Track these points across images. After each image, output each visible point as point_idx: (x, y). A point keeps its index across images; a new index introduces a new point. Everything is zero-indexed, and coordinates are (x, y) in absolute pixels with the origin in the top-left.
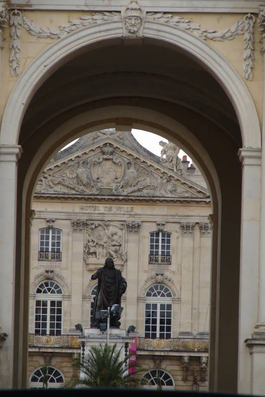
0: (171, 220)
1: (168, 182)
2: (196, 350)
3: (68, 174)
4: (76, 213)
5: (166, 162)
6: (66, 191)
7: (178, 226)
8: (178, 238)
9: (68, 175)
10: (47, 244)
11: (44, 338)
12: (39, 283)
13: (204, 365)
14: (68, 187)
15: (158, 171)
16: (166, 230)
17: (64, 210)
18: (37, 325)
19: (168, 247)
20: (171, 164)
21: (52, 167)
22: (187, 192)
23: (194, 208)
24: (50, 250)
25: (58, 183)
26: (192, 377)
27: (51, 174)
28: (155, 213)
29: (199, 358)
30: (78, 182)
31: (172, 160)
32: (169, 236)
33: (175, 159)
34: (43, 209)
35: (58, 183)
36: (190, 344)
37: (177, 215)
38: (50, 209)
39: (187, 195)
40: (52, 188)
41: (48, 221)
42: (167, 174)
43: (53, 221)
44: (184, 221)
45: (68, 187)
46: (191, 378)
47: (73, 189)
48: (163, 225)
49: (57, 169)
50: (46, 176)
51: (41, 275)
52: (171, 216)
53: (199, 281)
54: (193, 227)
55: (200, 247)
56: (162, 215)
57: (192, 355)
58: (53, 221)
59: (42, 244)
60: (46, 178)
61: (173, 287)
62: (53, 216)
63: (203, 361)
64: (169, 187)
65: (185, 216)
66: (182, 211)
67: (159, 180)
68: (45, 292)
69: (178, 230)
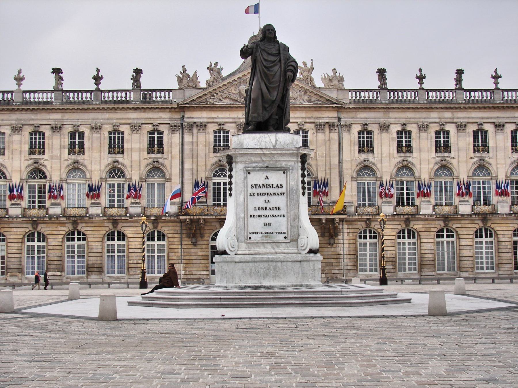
0: (308, 121)
1: (305, 94)
2: (331, 213)
3: (233, 90)
4: (239, 118)
5: (303, 80)
6: (232, 102)
7: (313, 125)
8: (313, 134)
9: (233, 91)
10: (220, 141)
11: (219, 209)
12: (214, 169)
13: (337, 224)
14: (233, 100)
15: (297, 86)
16: (304, 128)
17: (231, 116)
18: (214, 200)
19: (307, 141)
20: (306, 81)
21: (221, 85)
22: (319, 100)
23: (324, 112)
24: (222, 145)
25: (226, 97)
26: (328, 234)
27: (221, 91)
28: (296, 116)
29: (334, 219)
30: (240, 96)
31: (307, 79)
32: (307, 132)
33: (309, 78)
34: (216, 116)
35: (226, 97)
36: (327, 209)
37: (312, 117)
38: (220, 116)
39: (319, 103)
40: (222, 100)
41: (219, 125)
42: (304, 88)
43: (223, 125)
44: (318, 121)
45: (233, 100)
46: (327, 234)
47: (237, 101)
48: (303, 124)
49: (225, 87)
50: (217, 92)
51: (216, 163)
52: (308, 118)
53: (330, 164)
54: (324, 125)
55: (330, 140)
56: (301, 118)
57: (328, 217)
58: (223, 125)
59: (216, 141)
60: (217, 94)
61: (311, 169)
62: (224, 121)
63: (336, 222)
64: (306, 98)
65: (318, 118)
66: (316, 114)
67: (299, 93)
68: (219, 176)
69: (314, 128)
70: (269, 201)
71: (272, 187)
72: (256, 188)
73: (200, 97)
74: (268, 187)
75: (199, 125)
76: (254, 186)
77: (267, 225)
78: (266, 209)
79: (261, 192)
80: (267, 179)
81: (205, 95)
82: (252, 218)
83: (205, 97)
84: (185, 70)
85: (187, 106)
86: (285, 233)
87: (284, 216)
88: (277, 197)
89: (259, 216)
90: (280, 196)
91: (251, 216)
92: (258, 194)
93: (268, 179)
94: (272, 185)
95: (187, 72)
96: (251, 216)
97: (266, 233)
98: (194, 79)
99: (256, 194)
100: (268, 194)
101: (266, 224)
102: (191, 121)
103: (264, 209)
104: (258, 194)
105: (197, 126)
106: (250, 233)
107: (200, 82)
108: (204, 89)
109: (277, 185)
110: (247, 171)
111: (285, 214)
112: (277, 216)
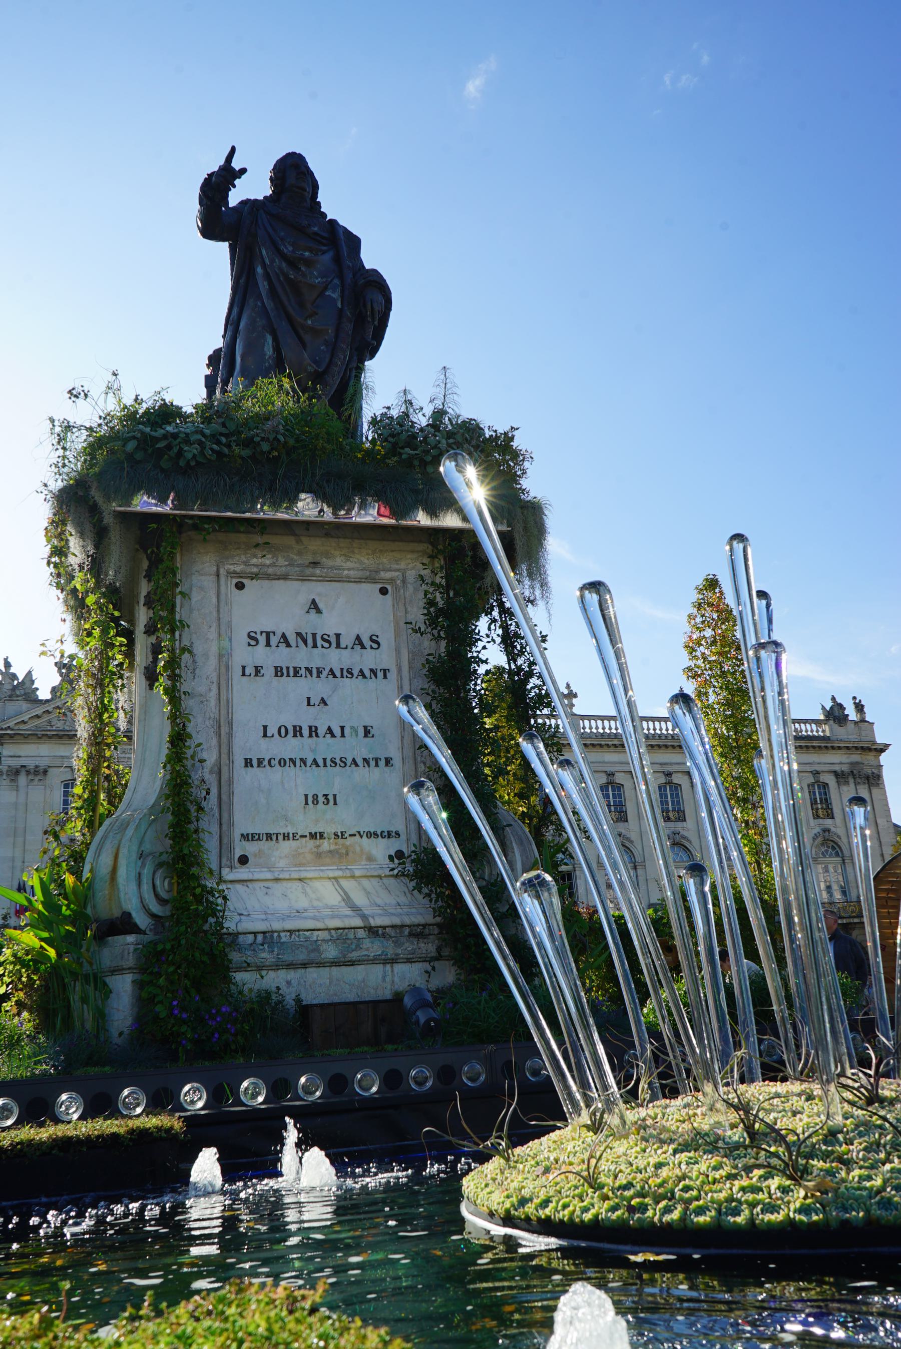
70: (324, 702)
71: (338, 646)
72: (268, 644)
73: (38, 716)
74: (319, 642)
75: (32, 771)
76: (262, 639)
77: (321, 799)
78: (313, 731)
79: (291, 666)
80: (313, 611)
81: (48, 712)
82: (255, 770)
83: (46, 718)
84: (7, 665)
85: (9, 732)
86: (398, 834)
87: (388, 762)
88: (356, 683)
89: (282, 763)
90: (372, 683)
91: (248, 763)
92: (278, 672)
93: (319, 611)
94: (338, 636)
95: (12, 670)
96: (248, 763)
97: (313, 836)
98: (28, 684)
99: (268, 672)
100: (319, 672)
101: (315, 797)
102: (16, 763)
103: (306, 732)
104: (278, 672)
105: (28, 772)
106: (245, 837)
107: (37, 689)
108: (47, 701)
109: (358, 638)
110: (231, 574)
111: (394, 753)
112: (360, 762)
